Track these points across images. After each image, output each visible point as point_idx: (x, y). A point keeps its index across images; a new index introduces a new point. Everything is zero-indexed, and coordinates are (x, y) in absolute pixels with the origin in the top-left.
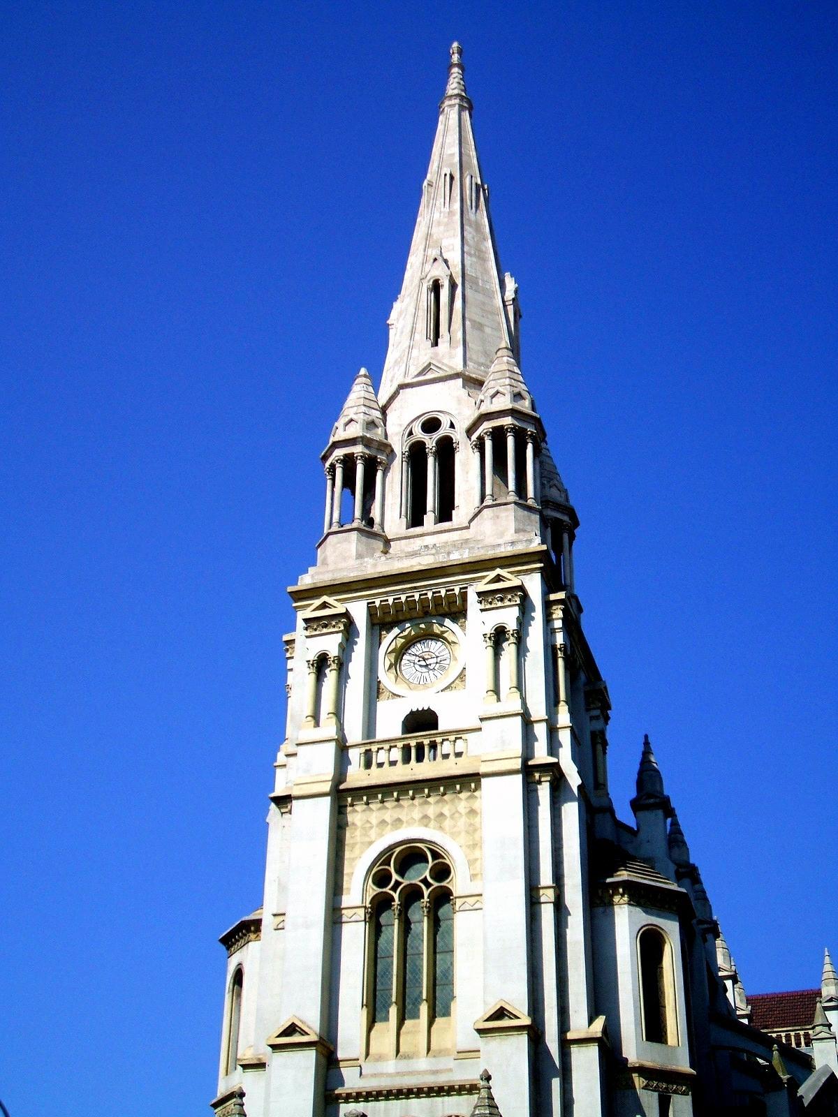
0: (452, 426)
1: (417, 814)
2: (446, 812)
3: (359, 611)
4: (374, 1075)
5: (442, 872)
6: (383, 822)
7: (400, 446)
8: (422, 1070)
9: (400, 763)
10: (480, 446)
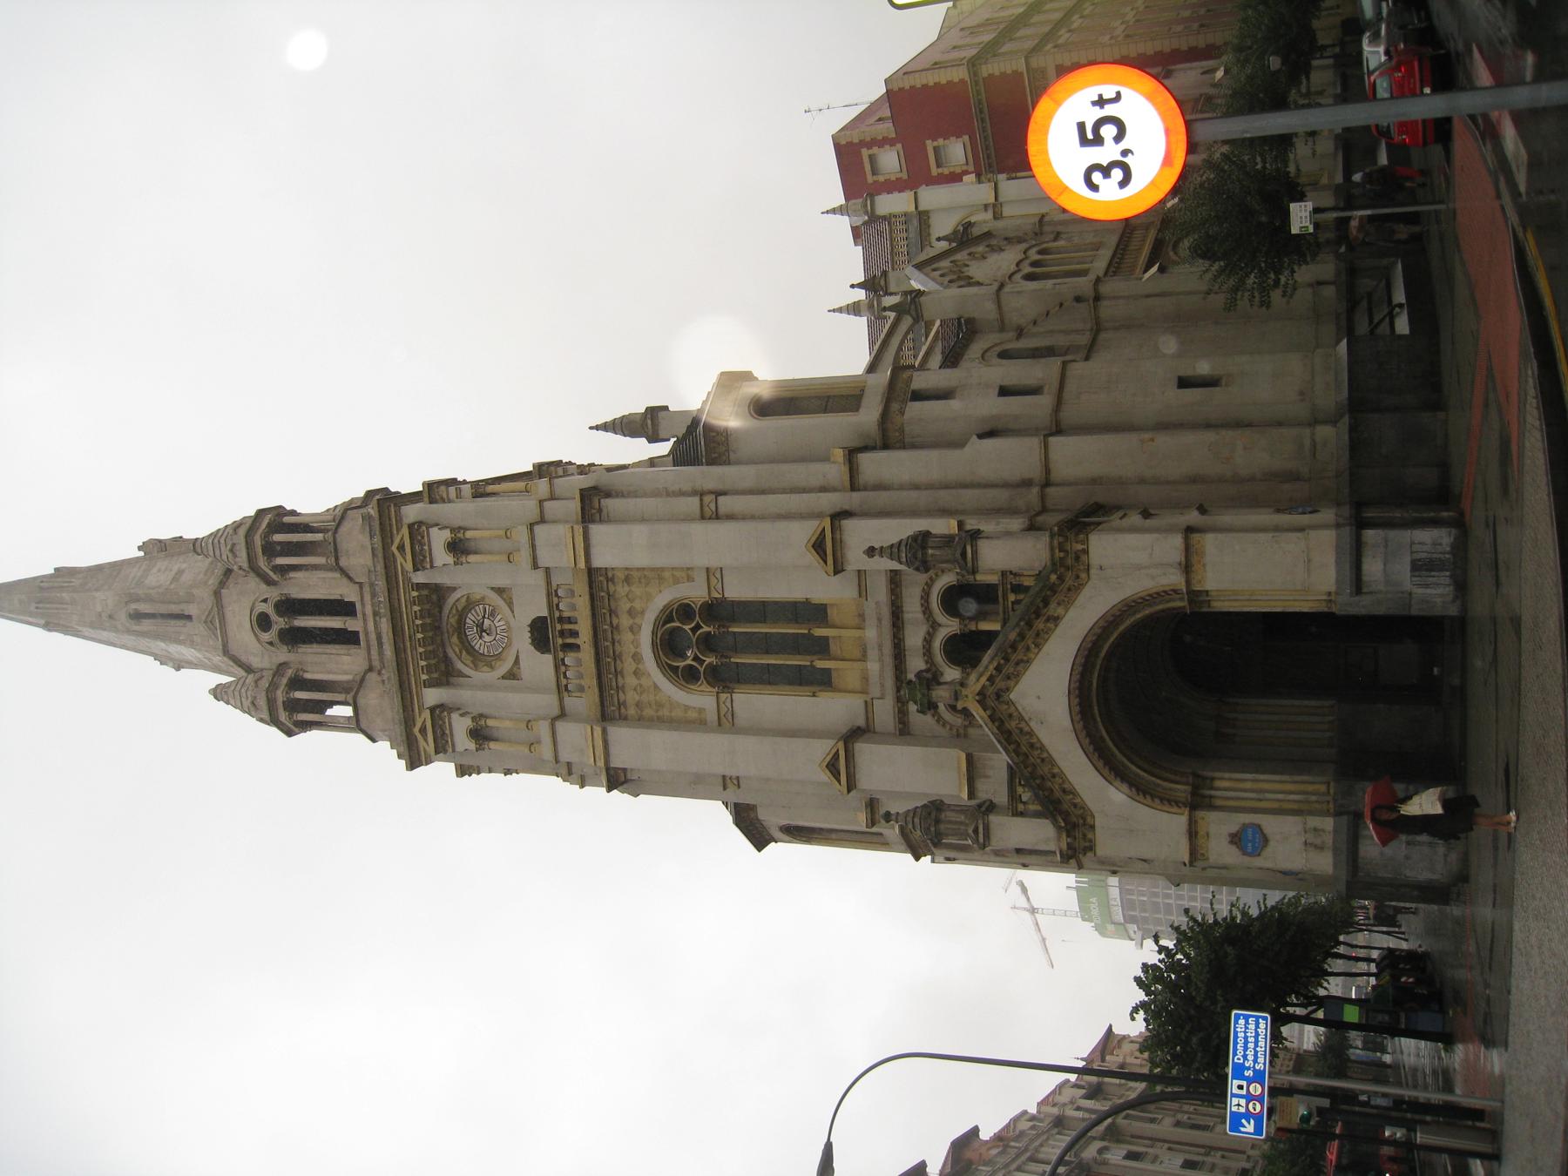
0: (265, 601)
1: (627, 637)
2: (628, 605)
3: (432, 696)
4: (882, 685)
5: (684, 611)
6: (635, 673)
7: (283, 654)
8: (875, 634)
9: (580, 655)
10: (284, 570)
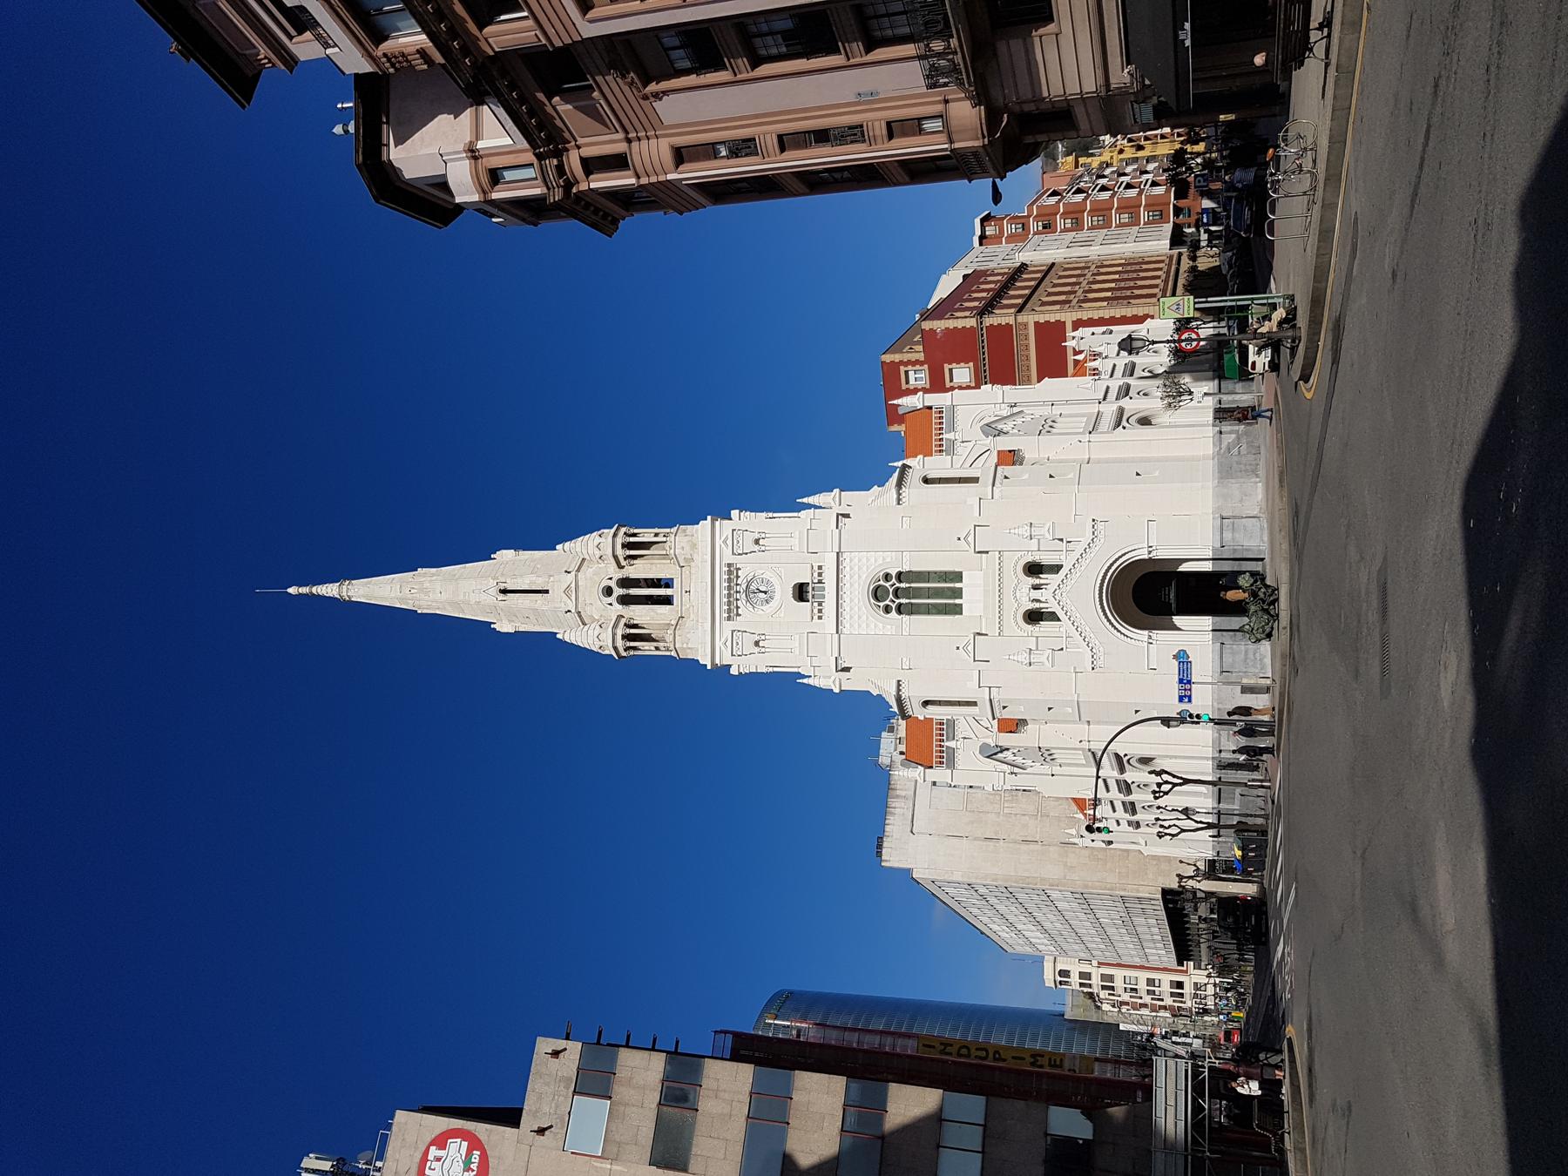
3: (729, 626)
7: (619, 608)
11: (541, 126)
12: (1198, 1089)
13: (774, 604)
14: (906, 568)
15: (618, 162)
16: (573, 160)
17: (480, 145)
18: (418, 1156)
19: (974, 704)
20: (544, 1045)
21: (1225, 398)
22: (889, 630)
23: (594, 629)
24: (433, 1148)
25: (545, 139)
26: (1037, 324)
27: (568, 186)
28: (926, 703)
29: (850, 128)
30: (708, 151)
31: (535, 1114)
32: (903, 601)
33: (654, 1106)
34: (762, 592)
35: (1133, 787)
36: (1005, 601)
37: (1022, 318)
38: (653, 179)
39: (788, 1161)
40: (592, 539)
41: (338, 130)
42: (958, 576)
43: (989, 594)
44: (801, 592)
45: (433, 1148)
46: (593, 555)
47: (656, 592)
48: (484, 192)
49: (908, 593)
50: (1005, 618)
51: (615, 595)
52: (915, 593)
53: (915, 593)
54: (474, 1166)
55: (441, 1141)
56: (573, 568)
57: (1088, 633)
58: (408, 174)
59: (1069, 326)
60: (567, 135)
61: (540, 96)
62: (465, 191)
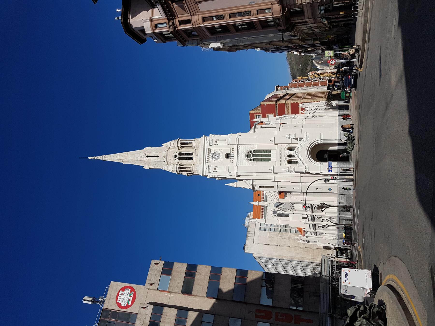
3: (208, 164)
11: (169, 11)
12: (333, 267)
13: (220, 159)
14: (256, 149)
15: (188, 22)
16: (177, 21)
17: (153, 18)
18: (117, 293)
19: (273, 187)
20: (153, 262)
21: (341, 113)
22: (251, 165)
23: (171, 166)
24: (121, 291)
25: (170, 14)
26: (291, 103)
27: (175, 28)
28: (260, 187)
29: (247, 12)
30: (211, 18)
31: (150, 280)
32: (255, 158)
33: (183, 277)
34: (216, 156)
35: (316, 217)
36: (282, 157)
37: (287, 102)
38: (197, 26)
39: (220, 290)
40: (173, 142)
41: (116, 18)
42: (270, 151)
43: (278, 156)
44: (227, 156)
45: (121, 291)
46: (172, 147)
47: (188, 156)
48: (153, 30)
49: (256, 155)
50: (282, 162)
51: (177, 157)
52: (259, 156)
53: (259, 156)
54: (132, 296)
55: (123, 289)
56: (166, 150)
57: (304, 163)
58: (134, 26)
59: (300, 103)
60: (175, 14)
61: (170, 2)
62: (148, 31)
